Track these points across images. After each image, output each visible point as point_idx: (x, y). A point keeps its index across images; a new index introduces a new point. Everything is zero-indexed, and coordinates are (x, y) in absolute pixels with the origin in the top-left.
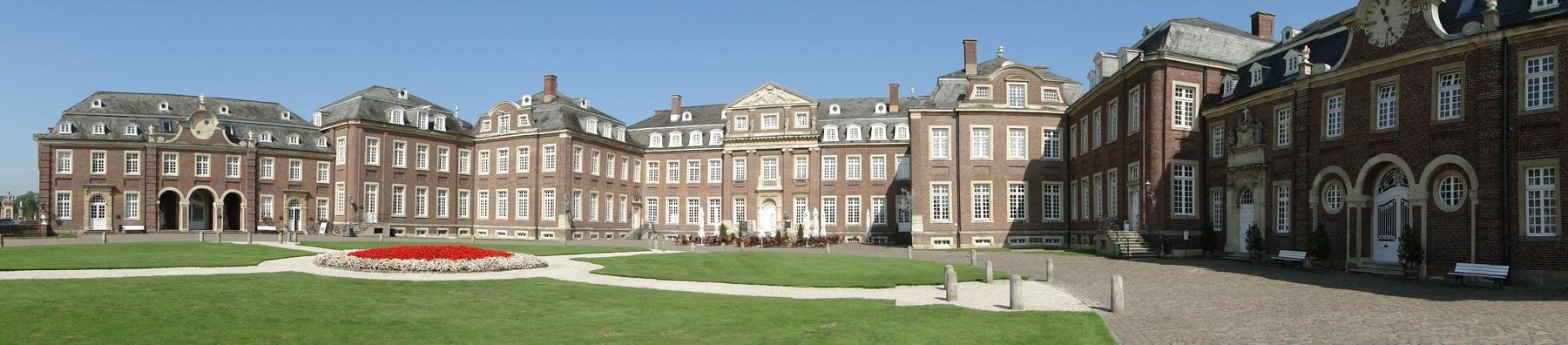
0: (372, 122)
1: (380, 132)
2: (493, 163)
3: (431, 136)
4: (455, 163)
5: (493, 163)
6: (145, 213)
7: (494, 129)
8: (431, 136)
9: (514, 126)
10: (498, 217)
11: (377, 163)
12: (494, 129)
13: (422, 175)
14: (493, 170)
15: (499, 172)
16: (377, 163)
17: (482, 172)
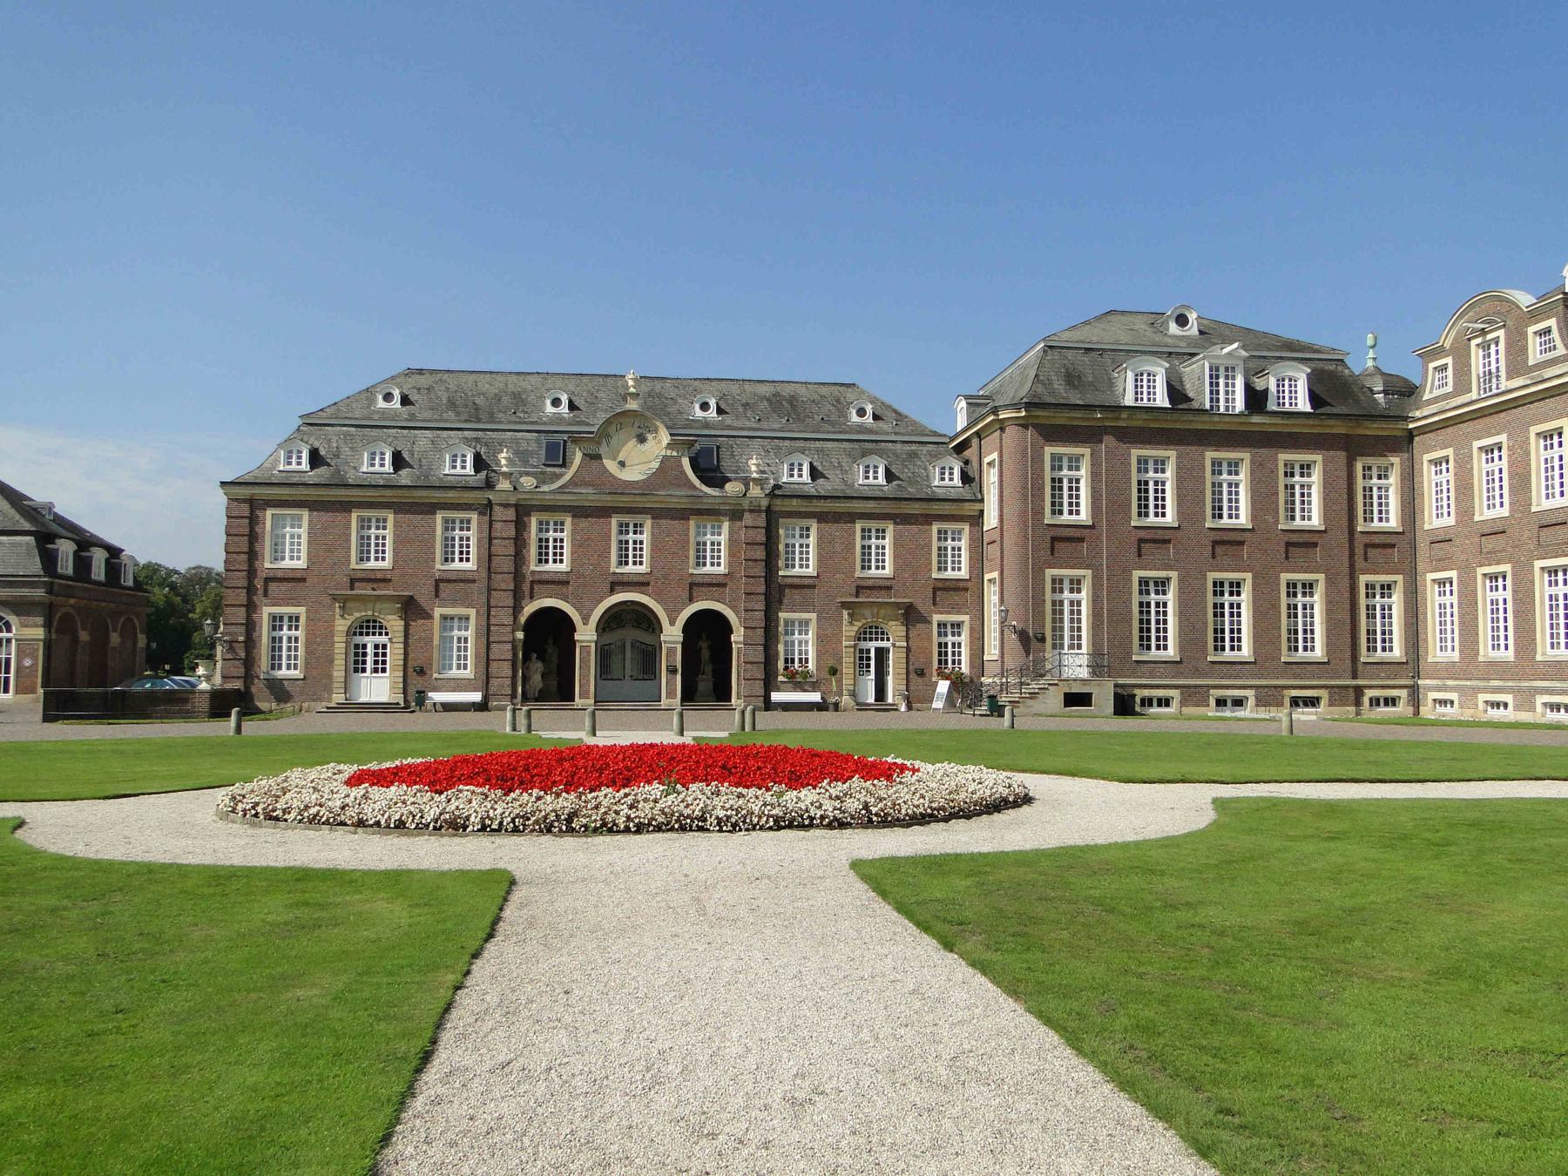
0: (1067, 411)
1: (1089, 435)
2: (1464, 488)
3: (1260, 430)
4: (1344, 501)
5: (1464, 488)
6: (486, 661)
7: (1462, 385)
8: (1260, 430)
9: (1517, 364)
10: (1486, 652)
11: (1084, 516)
12: (1462, 385)
13: (1227, 543)
14: (1465, 512)
15: (1485, 513)
16: (1084, 516)
17: (1436, 518)
